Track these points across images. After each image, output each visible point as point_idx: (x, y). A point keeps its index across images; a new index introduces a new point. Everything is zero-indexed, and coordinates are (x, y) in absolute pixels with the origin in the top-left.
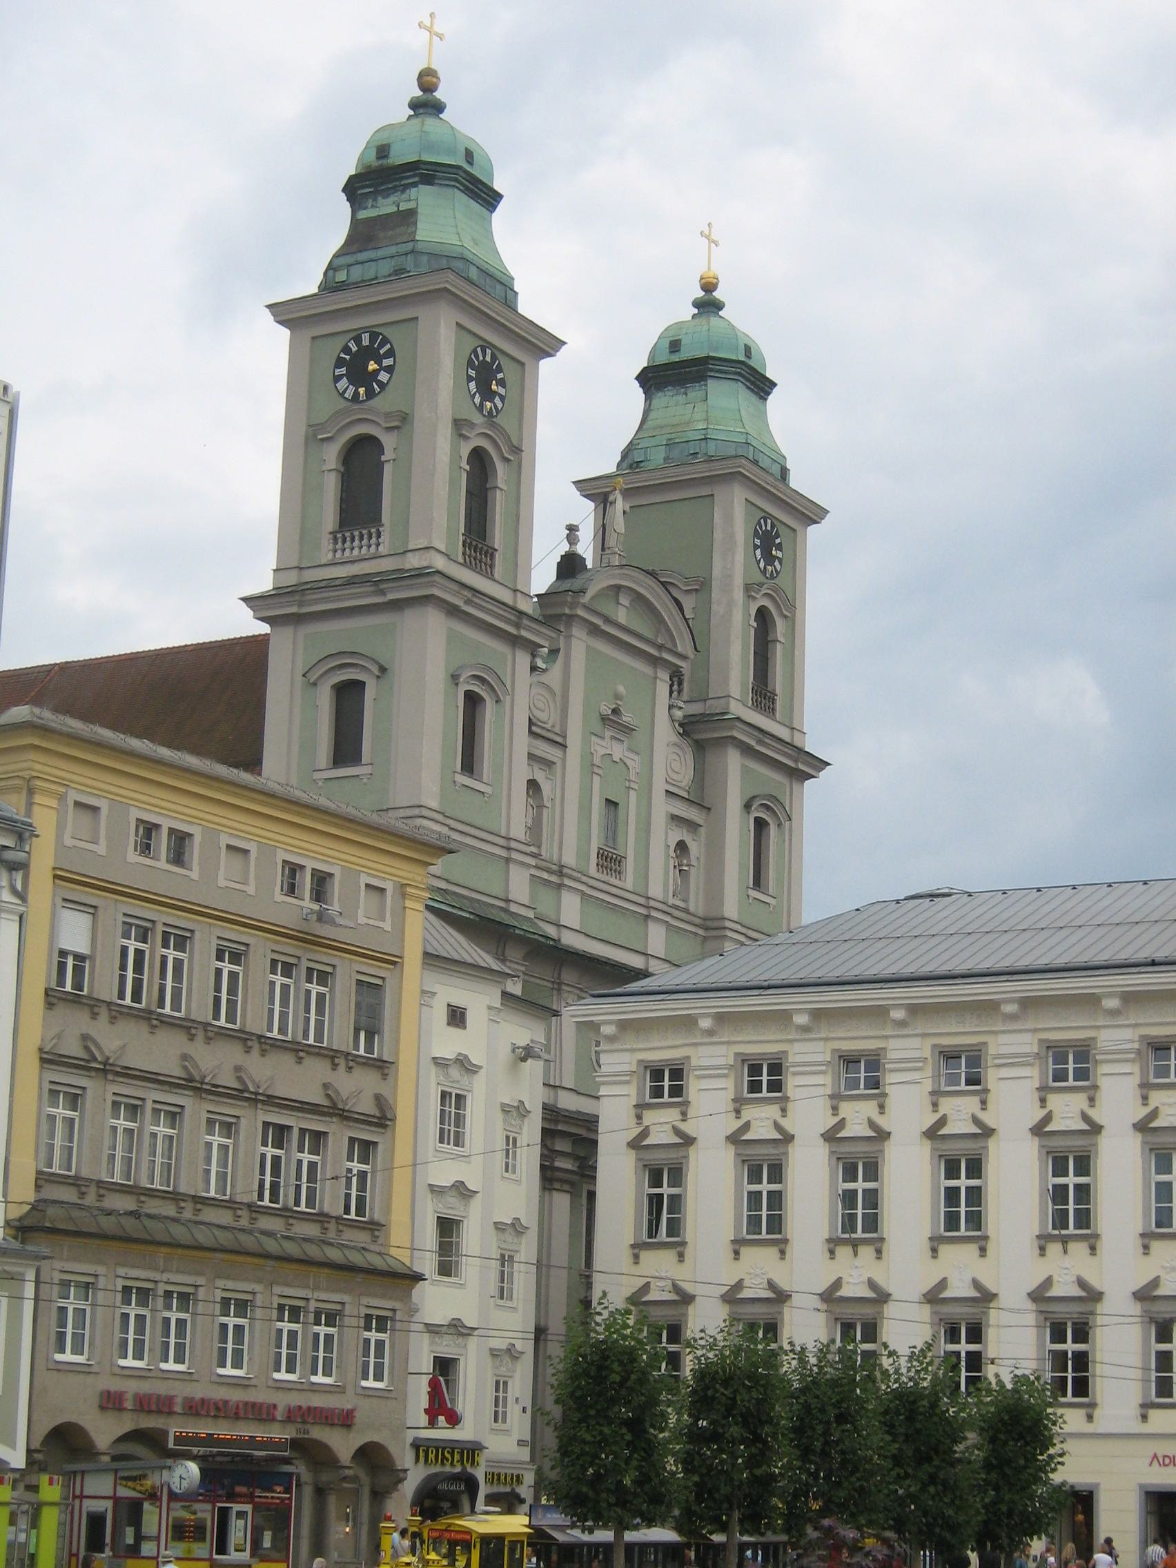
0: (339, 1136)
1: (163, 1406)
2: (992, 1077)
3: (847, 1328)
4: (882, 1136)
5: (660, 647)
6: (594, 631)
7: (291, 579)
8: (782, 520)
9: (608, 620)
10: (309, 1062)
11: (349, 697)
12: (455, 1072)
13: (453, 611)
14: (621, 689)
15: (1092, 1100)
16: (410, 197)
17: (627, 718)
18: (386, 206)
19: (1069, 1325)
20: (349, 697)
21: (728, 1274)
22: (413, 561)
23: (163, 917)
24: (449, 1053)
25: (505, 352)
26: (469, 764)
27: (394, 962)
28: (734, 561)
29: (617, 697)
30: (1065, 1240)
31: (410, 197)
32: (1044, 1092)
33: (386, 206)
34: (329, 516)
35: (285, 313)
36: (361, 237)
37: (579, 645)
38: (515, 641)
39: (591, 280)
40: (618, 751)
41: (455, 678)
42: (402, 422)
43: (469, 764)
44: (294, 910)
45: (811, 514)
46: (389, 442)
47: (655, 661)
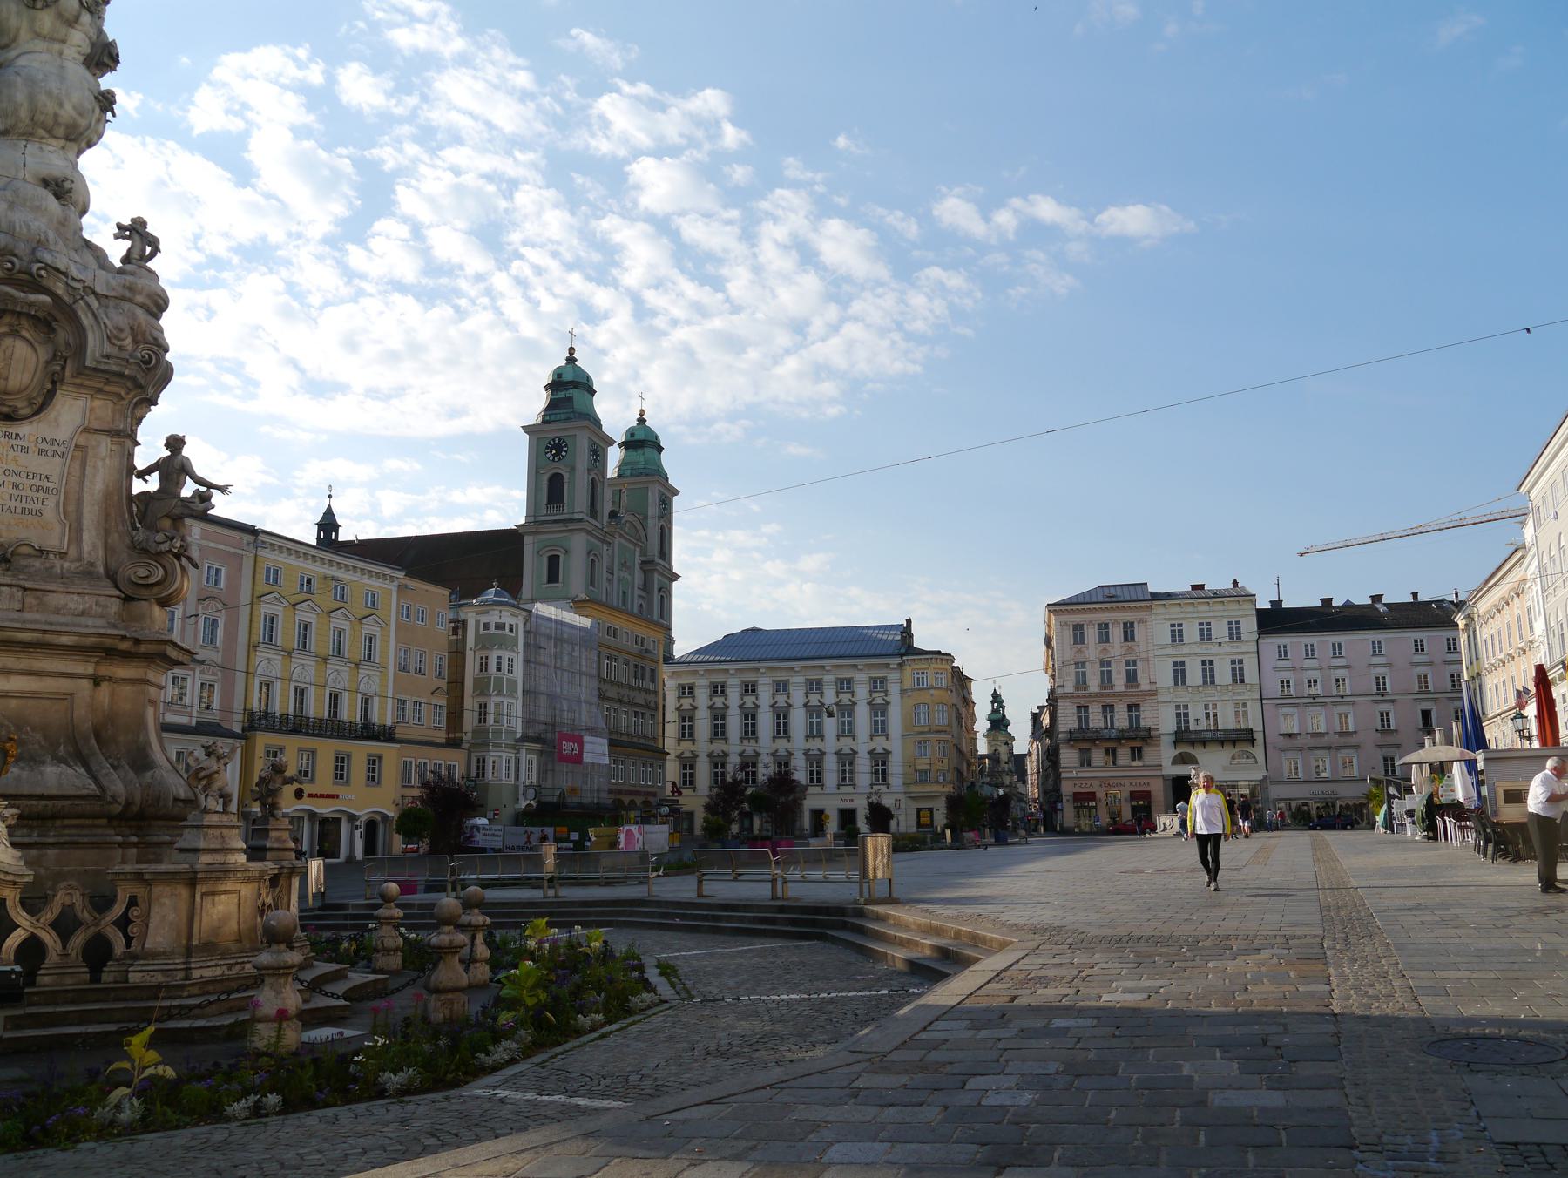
0: (648, 713)
1: (620, 792)
2: (791, 689)
3: (780, 765)
4: (757, 707)
8: (667, 495)
11: (553, 562)
13: (589, 533)
16: (569, 391)
18: (561, 395)
19: (815, 761)
20: (553, 562)
21: (738, 749)
22: (577, 516)
23: (613, 653)
25: (600, 444)
26: (592, 583)
27: (657, 662)
28: (653, 510)
31: (569, 391)
32: (807, 694)
33: (561, 395)
34: (545, 501)
35: (527, 429)
36: (552, 406)
38: (603, 541)
39: (614, 414)
41: (589, 553)
42: (572, 469)
43: (592, 583)
44: (636, 648)
45: (676, 492)
46: (566, 476)
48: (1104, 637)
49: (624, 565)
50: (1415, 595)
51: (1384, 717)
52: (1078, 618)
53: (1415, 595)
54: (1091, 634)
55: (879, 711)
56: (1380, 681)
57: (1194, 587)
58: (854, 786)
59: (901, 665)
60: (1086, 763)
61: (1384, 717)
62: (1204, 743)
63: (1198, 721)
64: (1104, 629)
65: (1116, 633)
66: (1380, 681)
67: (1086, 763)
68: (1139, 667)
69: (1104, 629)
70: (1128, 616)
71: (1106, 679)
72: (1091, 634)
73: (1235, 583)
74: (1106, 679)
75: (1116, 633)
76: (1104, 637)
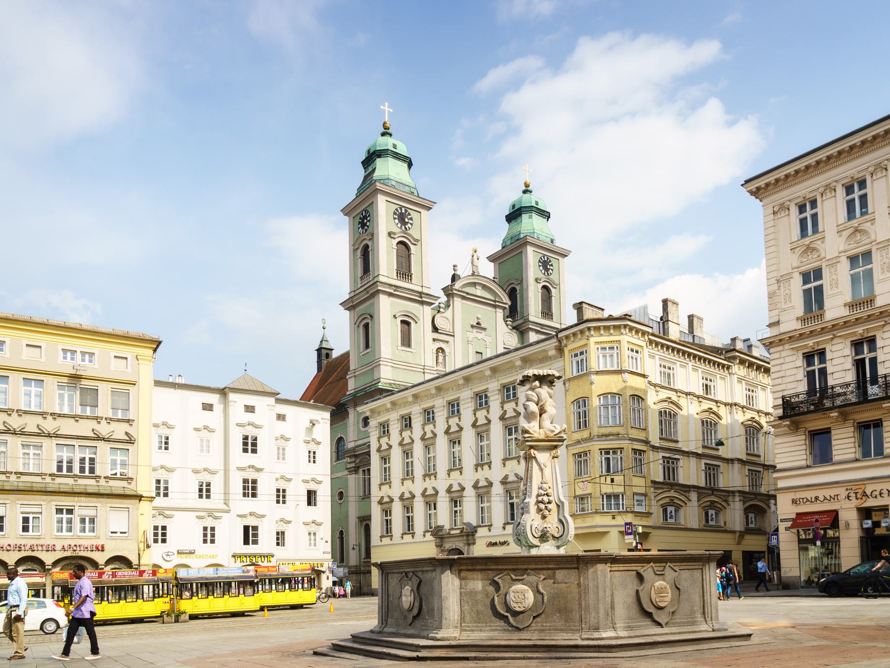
5: (495, 301)
6: (464, 298)
7: (353, 294)
9: (468, 294)
10: (81, 421)
11: (366, 326)
12: (250, 428)
14: (479, 316)
15: (488, 411)
17: (483, 326)
24: (245, 421)
29: (478, 318)
30: (482, 465)
37: (457, 301)
40: (480, 336)
41: (395, 316)
47: (495, 307)
49: (478, 326)
59: (560, 350)
60: (821, 453)
67: (821, 453)
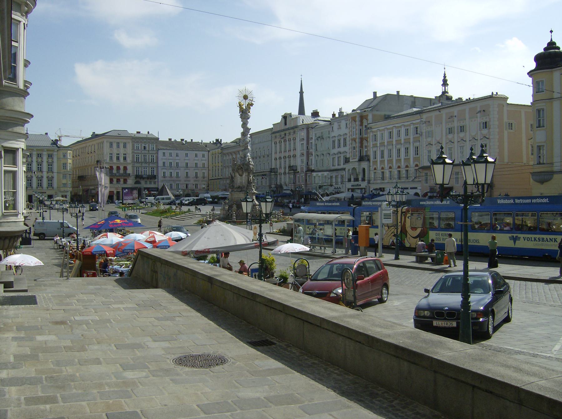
48: (118, 147)
50: (192, 140)
51: (187, 173)
52: (111, 140)
53: (192, 140)
54: (115, 145)
55: (50, 165)
56: (187, 164)
57: (138, 132)
58: (42, 188)
61: (187, 173)
62: (144, 178)
63: (142, 172)
64: (118, 143)
65: (121, 145)
66: (187, 164)
68: (127, 156)
69: (118, 143)
70: (125, 141)
71: (118, 158)
72: (115, 145)
73: (148, 132)
74: (118, 158)
75: (121, 145)
76: (118, 147)
